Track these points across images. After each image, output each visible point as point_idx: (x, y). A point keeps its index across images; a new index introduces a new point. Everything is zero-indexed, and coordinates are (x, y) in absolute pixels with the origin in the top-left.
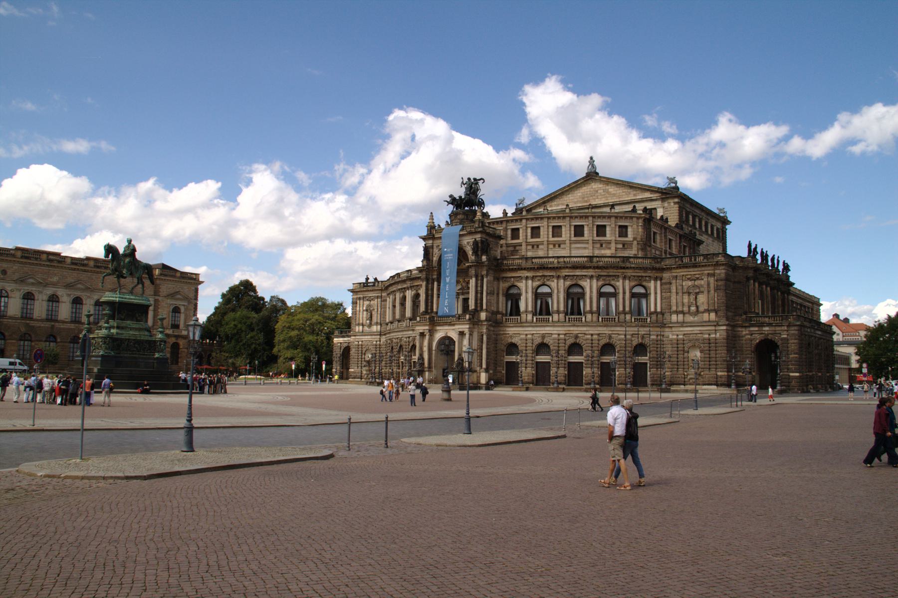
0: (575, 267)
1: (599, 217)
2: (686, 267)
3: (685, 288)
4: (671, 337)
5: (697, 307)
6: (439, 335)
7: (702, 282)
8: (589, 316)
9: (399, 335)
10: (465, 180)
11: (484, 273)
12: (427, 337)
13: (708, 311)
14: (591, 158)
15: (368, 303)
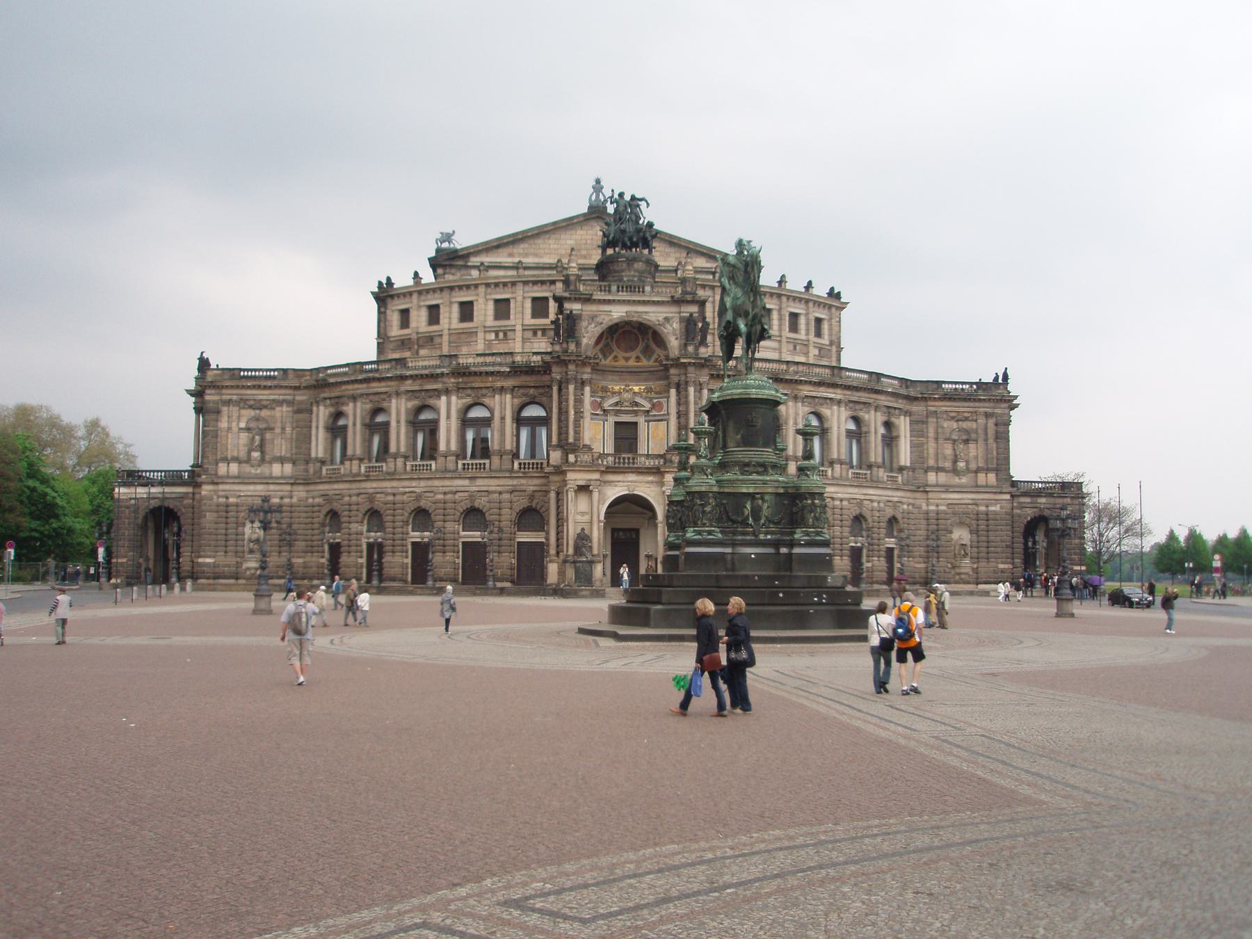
0: (820, 384)
1: (795, 299)
2: (954, 400)
3: (948, 431)
4: (924, 507)
5: (967, 462)
6: (613, 493)
7: (974, 425)
8: (837, 467)
9: (419, 486)
10: (616, 196)
11: (704, 378)
12: (596, 495)
13: (987, 470)
14: (598, 181)
15: (252, 413)
